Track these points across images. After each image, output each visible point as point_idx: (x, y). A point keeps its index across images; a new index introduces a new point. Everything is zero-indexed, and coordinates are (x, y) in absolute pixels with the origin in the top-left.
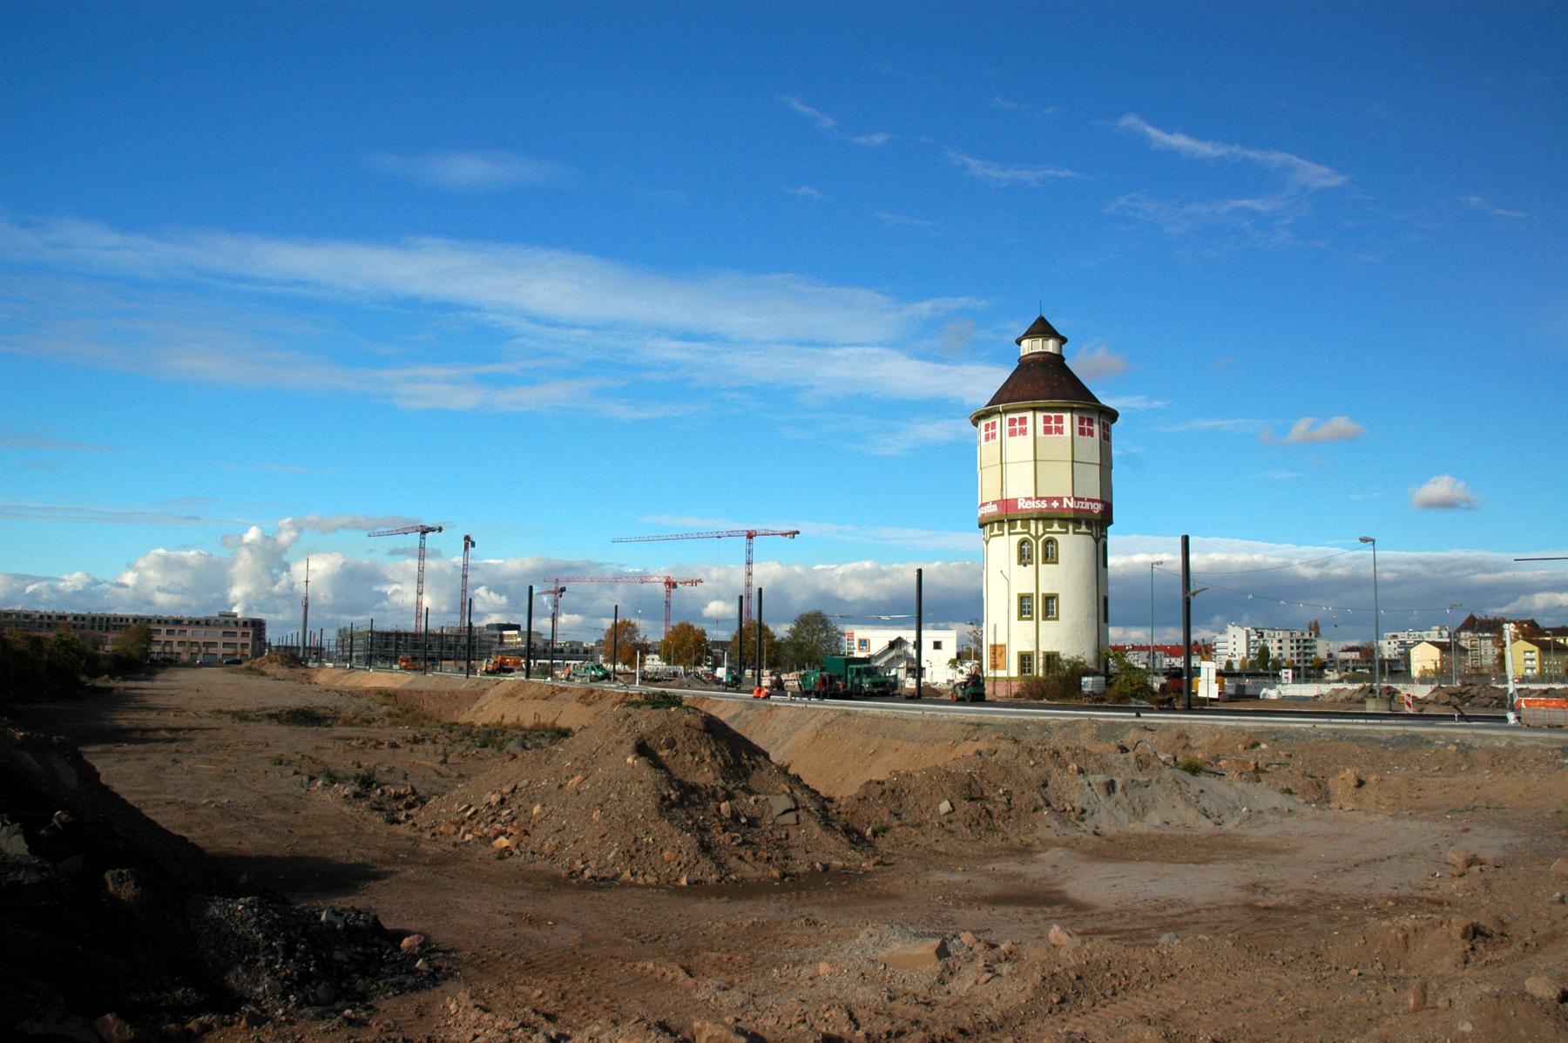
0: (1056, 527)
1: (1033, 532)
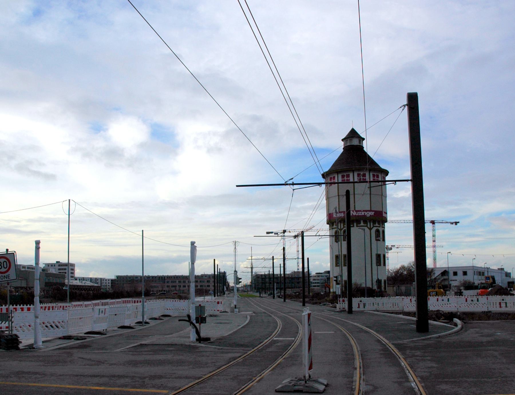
1: (339, 227)
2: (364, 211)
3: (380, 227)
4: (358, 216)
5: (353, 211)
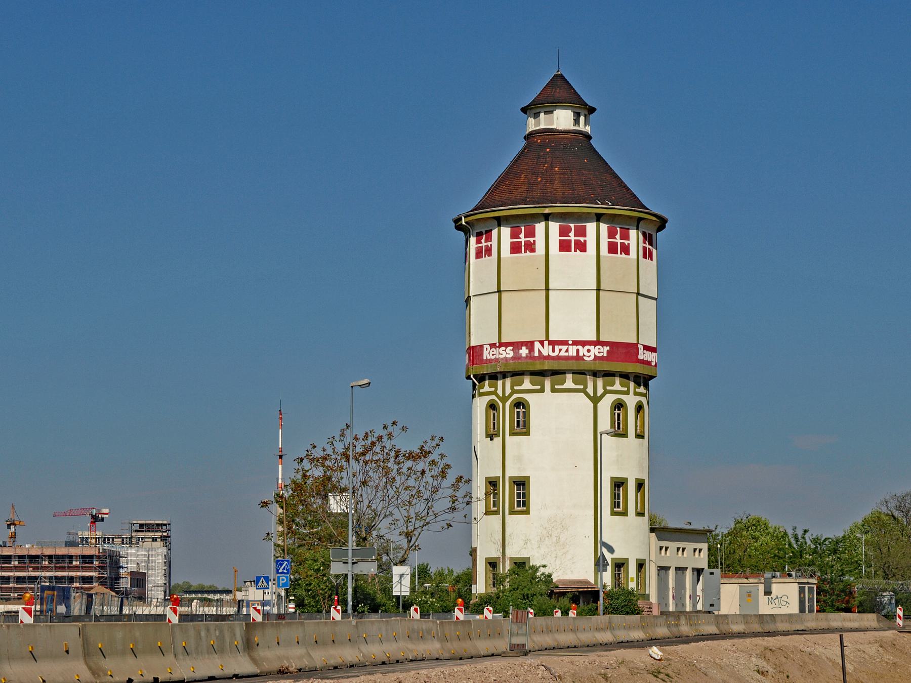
0: (527, 384)
1: (500, 392)
2: (575, 343)
3: (627, 393)
4: (558, 358)
5: (542, 343)
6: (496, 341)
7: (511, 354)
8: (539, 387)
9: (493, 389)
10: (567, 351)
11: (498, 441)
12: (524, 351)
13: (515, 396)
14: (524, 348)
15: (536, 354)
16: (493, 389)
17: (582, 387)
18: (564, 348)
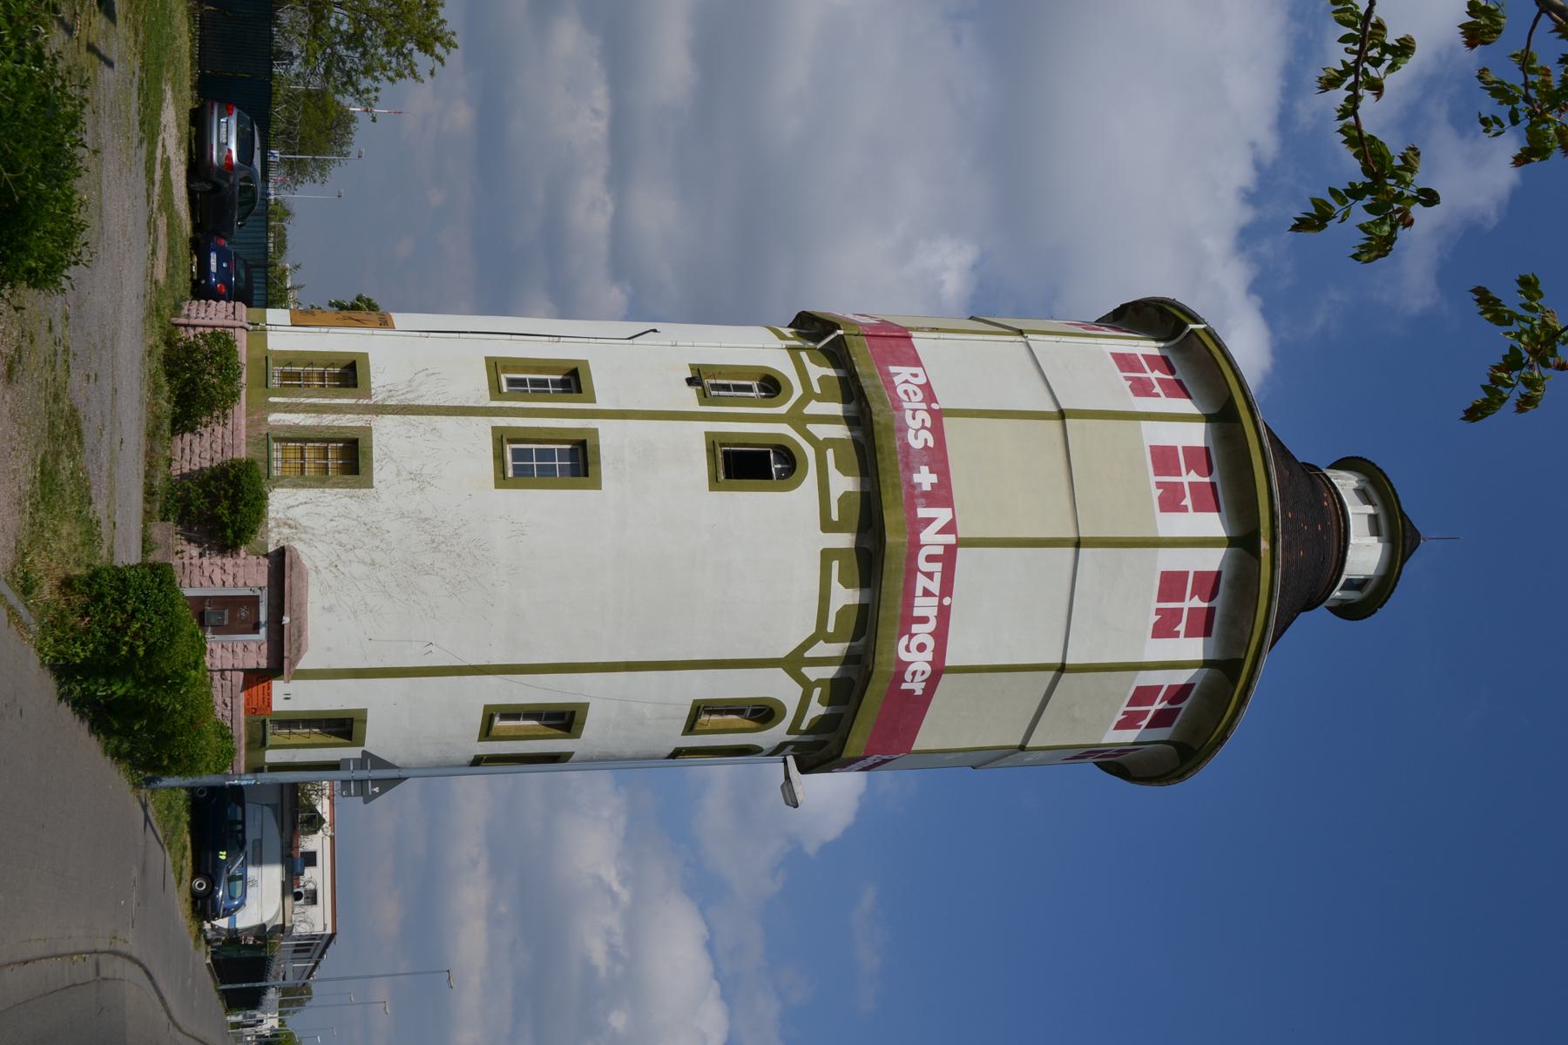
1: (814, 408)
2: (944, 614)
4: (912, 570)
5: (950, 528)
6: (943, 402)
7: (917, 444)
8: (835, 516)
9: (817, 389)
10: (927, 593)
11: (689, 399)
12: (925, 478)
13: (810, 451)
14: (934, 478)
15: (923, 513)
16: (817, 389)
17: (831, 629)
18: (935, 587)
